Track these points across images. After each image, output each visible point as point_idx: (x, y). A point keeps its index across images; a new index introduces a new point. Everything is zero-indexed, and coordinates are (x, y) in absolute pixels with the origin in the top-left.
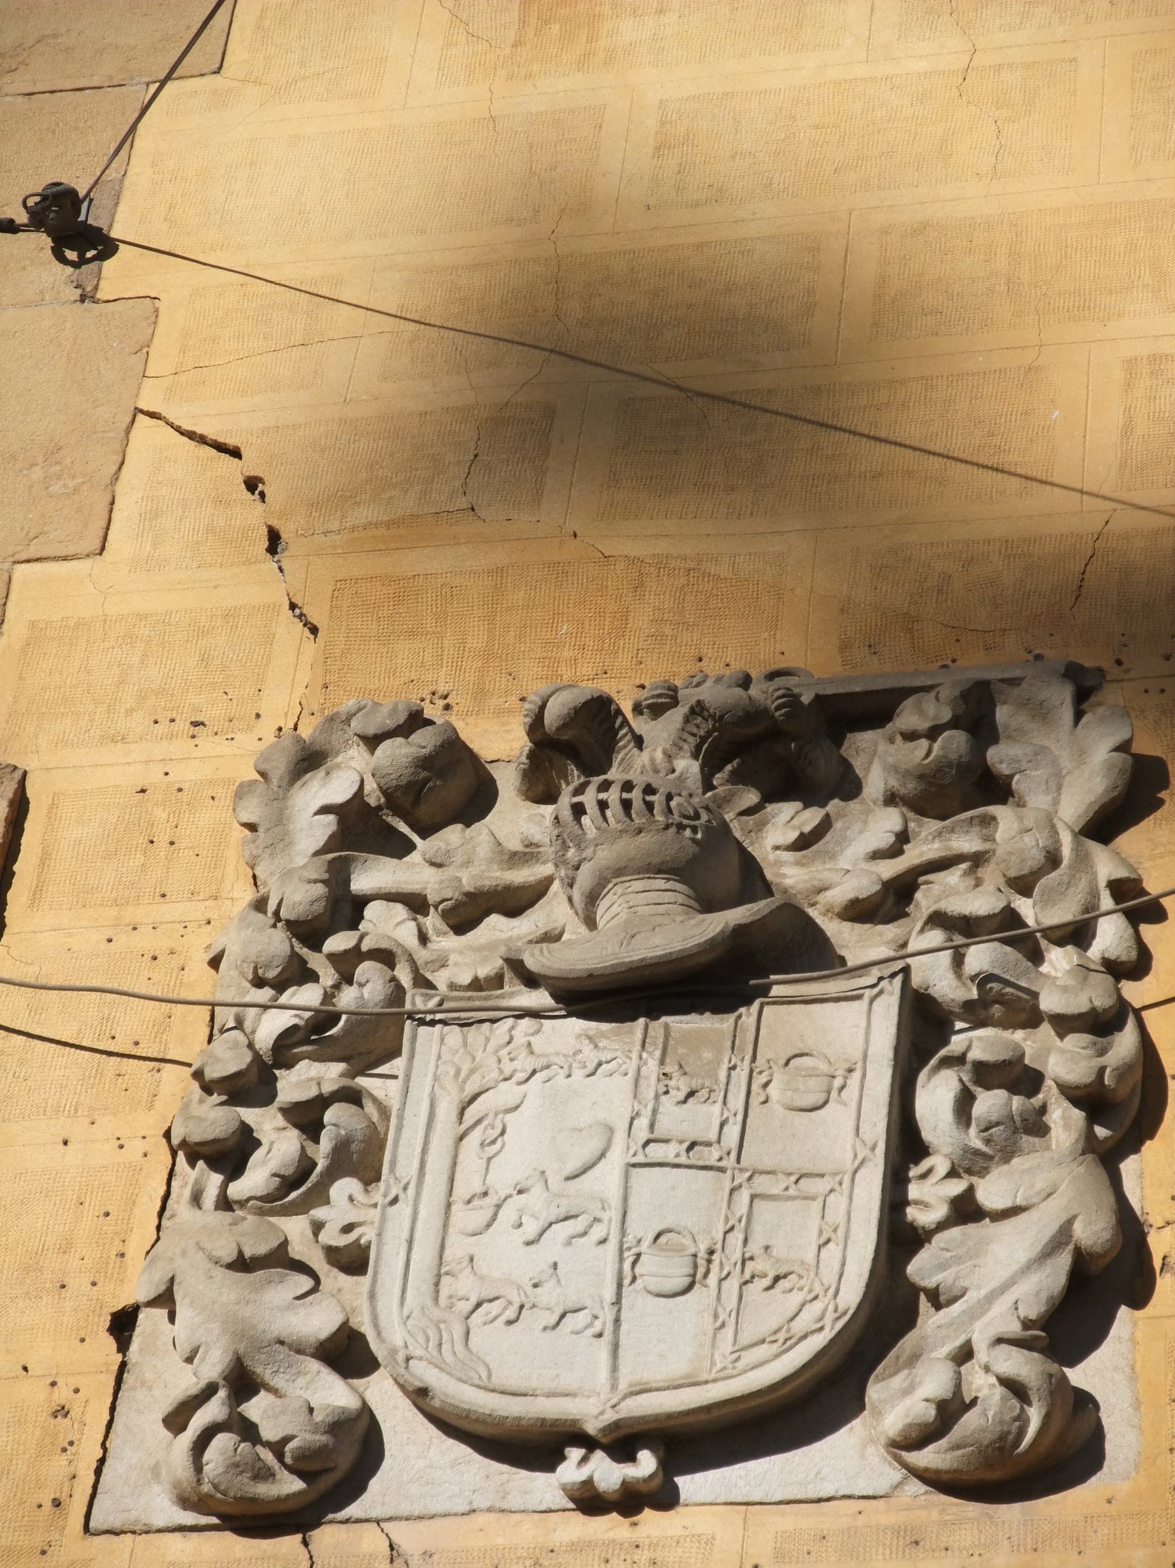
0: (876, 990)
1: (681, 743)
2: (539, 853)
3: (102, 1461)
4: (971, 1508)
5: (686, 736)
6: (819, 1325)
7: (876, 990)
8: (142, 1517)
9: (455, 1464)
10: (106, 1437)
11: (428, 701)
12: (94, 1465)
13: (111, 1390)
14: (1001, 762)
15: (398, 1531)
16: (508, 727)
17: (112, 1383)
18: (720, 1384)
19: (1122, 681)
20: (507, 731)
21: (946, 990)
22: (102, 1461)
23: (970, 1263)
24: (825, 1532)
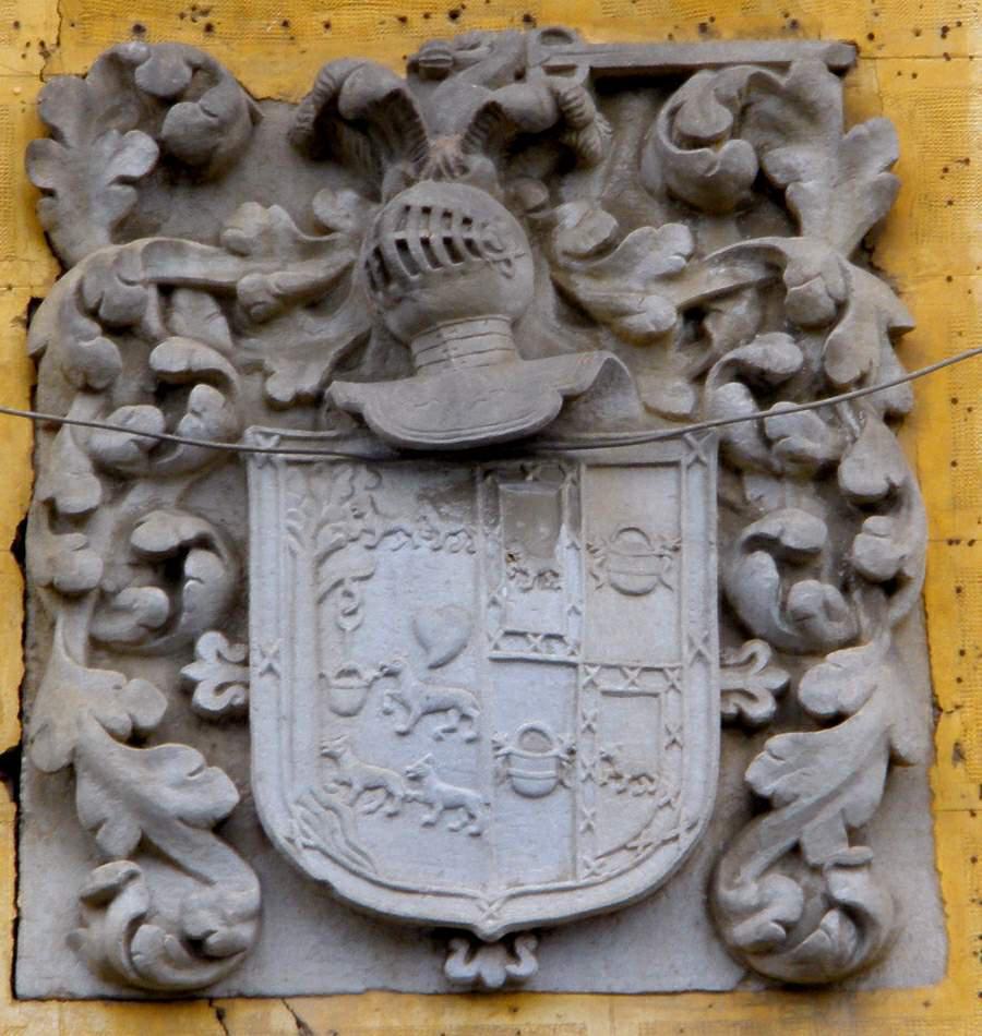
0: (675, 429)
1: (474, 138)
2: (334, 241)
3: (17, 922)
4: (496, 413)
5: (477, 131)
6: (672, 834)
7: (675, 429)
8: (65, 986)
9: (256, 710)
10: (16, 896)
11: (188, 18)
12: (10, 926)
13: (11, 844)
14: (776, 171)
15: (305, 1009)
16: (274, 58)
17: (11, 836)
18: (591, 892)
19: (875, 58)
20: (272, 63)
21: (747, 448)
22: (17, 922)
23: (799, 771)
24: (682, 1026)
